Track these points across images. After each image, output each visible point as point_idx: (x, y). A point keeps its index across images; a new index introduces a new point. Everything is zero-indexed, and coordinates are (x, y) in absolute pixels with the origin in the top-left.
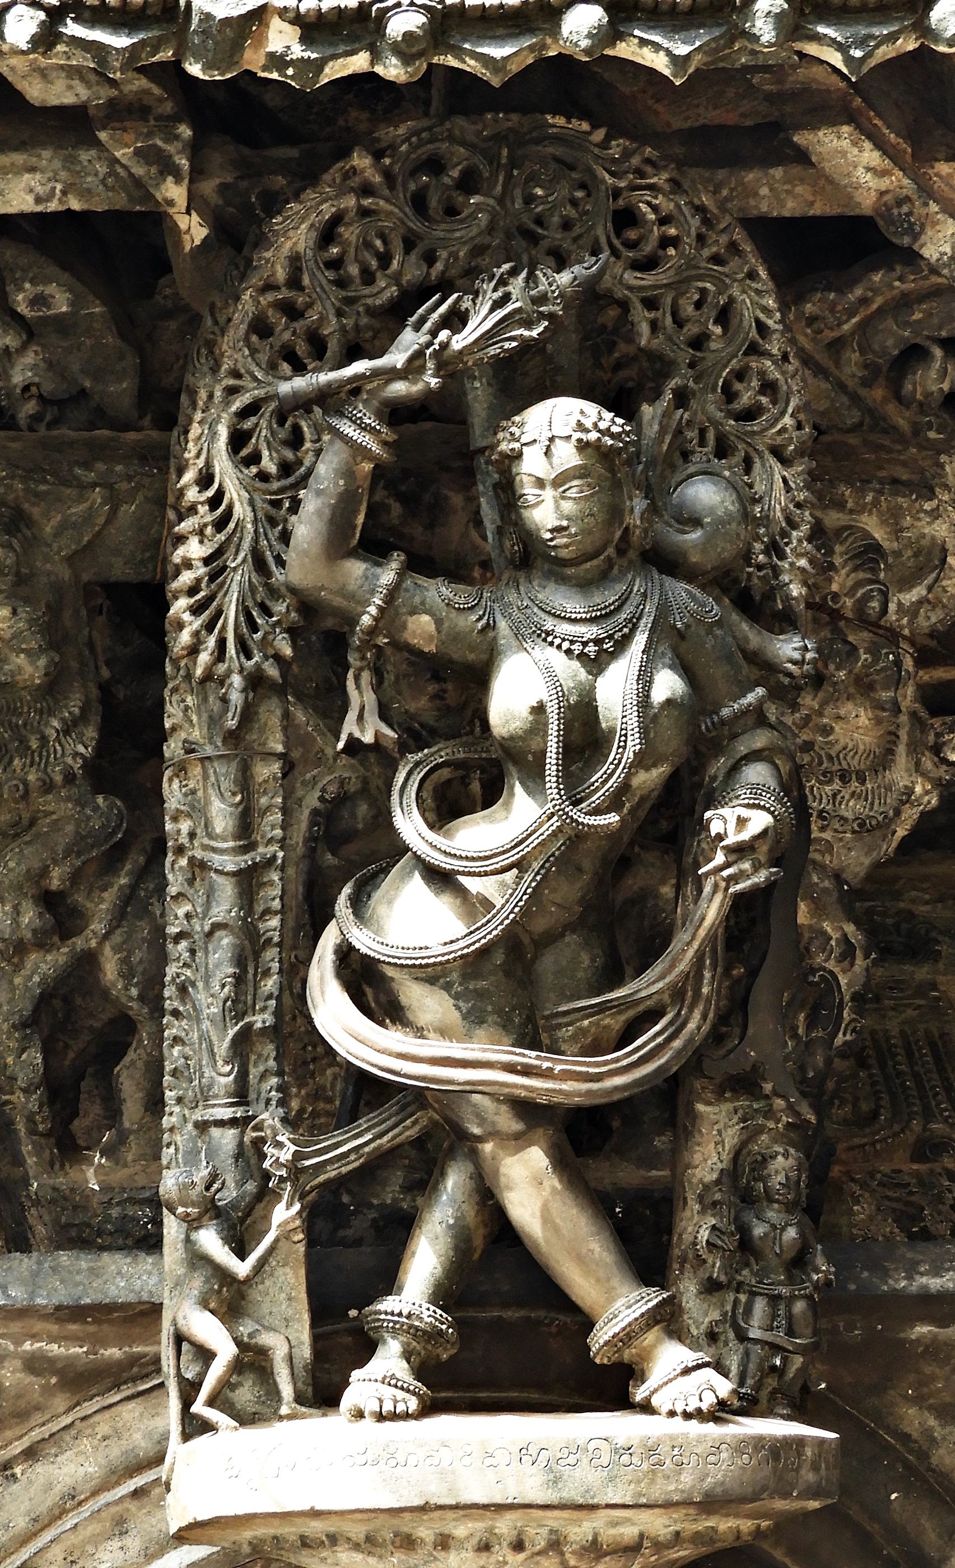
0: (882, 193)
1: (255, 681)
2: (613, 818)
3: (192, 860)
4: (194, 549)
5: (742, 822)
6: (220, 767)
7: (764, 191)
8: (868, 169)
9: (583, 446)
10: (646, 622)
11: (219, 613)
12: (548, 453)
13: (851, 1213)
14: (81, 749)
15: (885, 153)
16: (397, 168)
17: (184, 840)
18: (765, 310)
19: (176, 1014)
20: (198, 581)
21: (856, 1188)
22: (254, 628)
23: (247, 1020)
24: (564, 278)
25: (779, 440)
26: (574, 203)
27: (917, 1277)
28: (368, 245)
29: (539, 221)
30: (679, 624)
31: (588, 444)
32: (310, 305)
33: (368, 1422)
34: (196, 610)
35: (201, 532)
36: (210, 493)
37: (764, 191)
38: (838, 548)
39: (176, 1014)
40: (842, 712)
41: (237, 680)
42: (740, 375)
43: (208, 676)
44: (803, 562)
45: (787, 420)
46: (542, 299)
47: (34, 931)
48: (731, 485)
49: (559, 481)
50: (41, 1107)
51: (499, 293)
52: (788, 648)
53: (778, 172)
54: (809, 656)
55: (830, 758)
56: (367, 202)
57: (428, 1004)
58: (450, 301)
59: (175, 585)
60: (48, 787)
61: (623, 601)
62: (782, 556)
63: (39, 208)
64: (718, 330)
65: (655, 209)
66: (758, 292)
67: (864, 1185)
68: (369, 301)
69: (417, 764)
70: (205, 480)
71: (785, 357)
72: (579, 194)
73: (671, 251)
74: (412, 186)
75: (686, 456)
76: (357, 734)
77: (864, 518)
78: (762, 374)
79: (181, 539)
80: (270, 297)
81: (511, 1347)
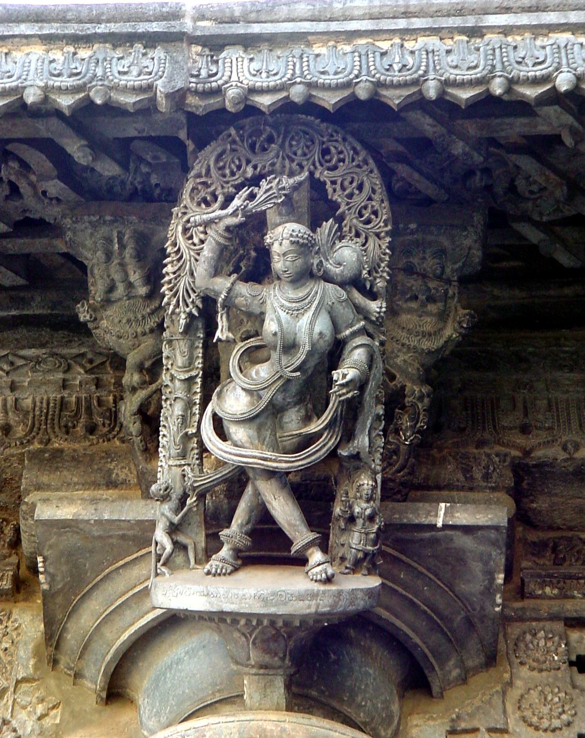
0: (435, 133)
1: (190, 315)
2: (298, 374)
3: (171, 374)
4: (169, 269)
5: (344, 376)
6: (181, 343)
7: (395, 130)
8: (428, 125)
9: (292, 243)
10: (316, 302)
11: (177, 291)
12: (281, 244)
13: (446, 469)
14: (157, 320)
15: (435, 119)
16: (246, 135)
17: (169, 367)
18: (375, 184)
19: (164, 426)
20: (171, 280)
21: (451, 458)
22: (190, 297)
23: (187, 430)
24: (291, 181)
25: (378, 231)
26: (308, 147)
27: (429, 517)
28: (234, 162)
29: (295, 154)
30: (329, 303)
31: (294, 242)
32: (212, 184)
33: (210, 576)
34: (171, 290)
35: (172, 262)
36: (176, 249)
37: (395, 130)
38: (428, 251)
39: (164, 426)
40: (425, 310)
41: (183, 316)
42: (365, 207)
43: (173, 313)
44: (385, 274)
45: (382, 224)
46: (284, 189)
47: (138, 384)
48: (354, 251)
49: (284, 254)
50: (141, 441)
51: (268, 187)
52: (375, 307)
53: (399, 124)
54: (384, 309)
55: (420, 326)
56: (233, 146)
57: (238, 433)
58: (250, 189)
59: (162, 281)
60: (144, 334)
61: (308, 294)
62: (377, 272)
63: (139, 135)
64: (357, 192)
65: (335, 147)
66: (373, 178)
67: (454, 458)
68: (233, 183)
69: (242, 347)
70: (174, 244)
71: (382, 201)
72: (309, 143)
73: (341, 164)
74: (250, 141)
75: (341, 238)
76: (220, 337)
77: (441, 237)
78: (373, 206)
79: (166, 265)
80: (198, 180)
81: (267, 547)
